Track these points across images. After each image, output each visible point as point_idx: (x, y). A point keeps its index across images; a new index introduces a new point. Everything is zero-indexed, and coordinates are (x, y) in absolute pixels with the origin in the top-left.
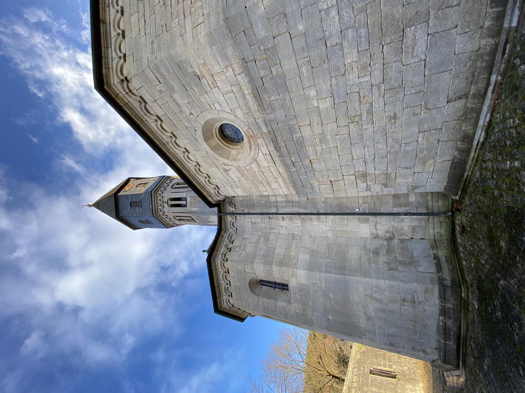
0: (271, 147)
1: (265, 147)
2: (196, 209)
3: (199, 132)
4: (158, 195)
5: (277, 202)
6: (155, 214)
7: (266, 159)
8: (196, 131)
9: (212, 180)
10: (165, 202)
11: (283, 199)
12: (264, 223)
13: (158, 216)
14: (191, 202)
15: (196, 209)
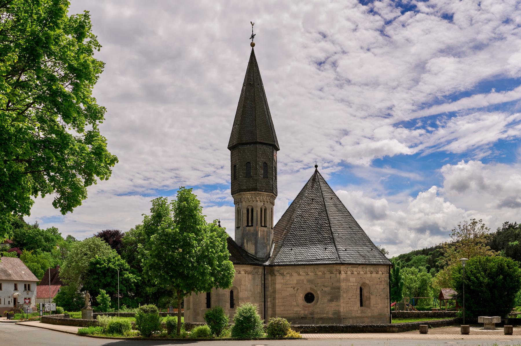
0: (302, 316)
1: (303, 313)
2: (260, 236)
3: (315, 288)
4: (269, 198)
5: (268, 302)
6: (258, 193)
7: (297, 311)
8: (316, 287)
9: (288, 275)
10: (264, 204)
11: (269, 305)
12: (257, 294)
13: (255, 193)
14: (264, 231)
15: (260, 236)
